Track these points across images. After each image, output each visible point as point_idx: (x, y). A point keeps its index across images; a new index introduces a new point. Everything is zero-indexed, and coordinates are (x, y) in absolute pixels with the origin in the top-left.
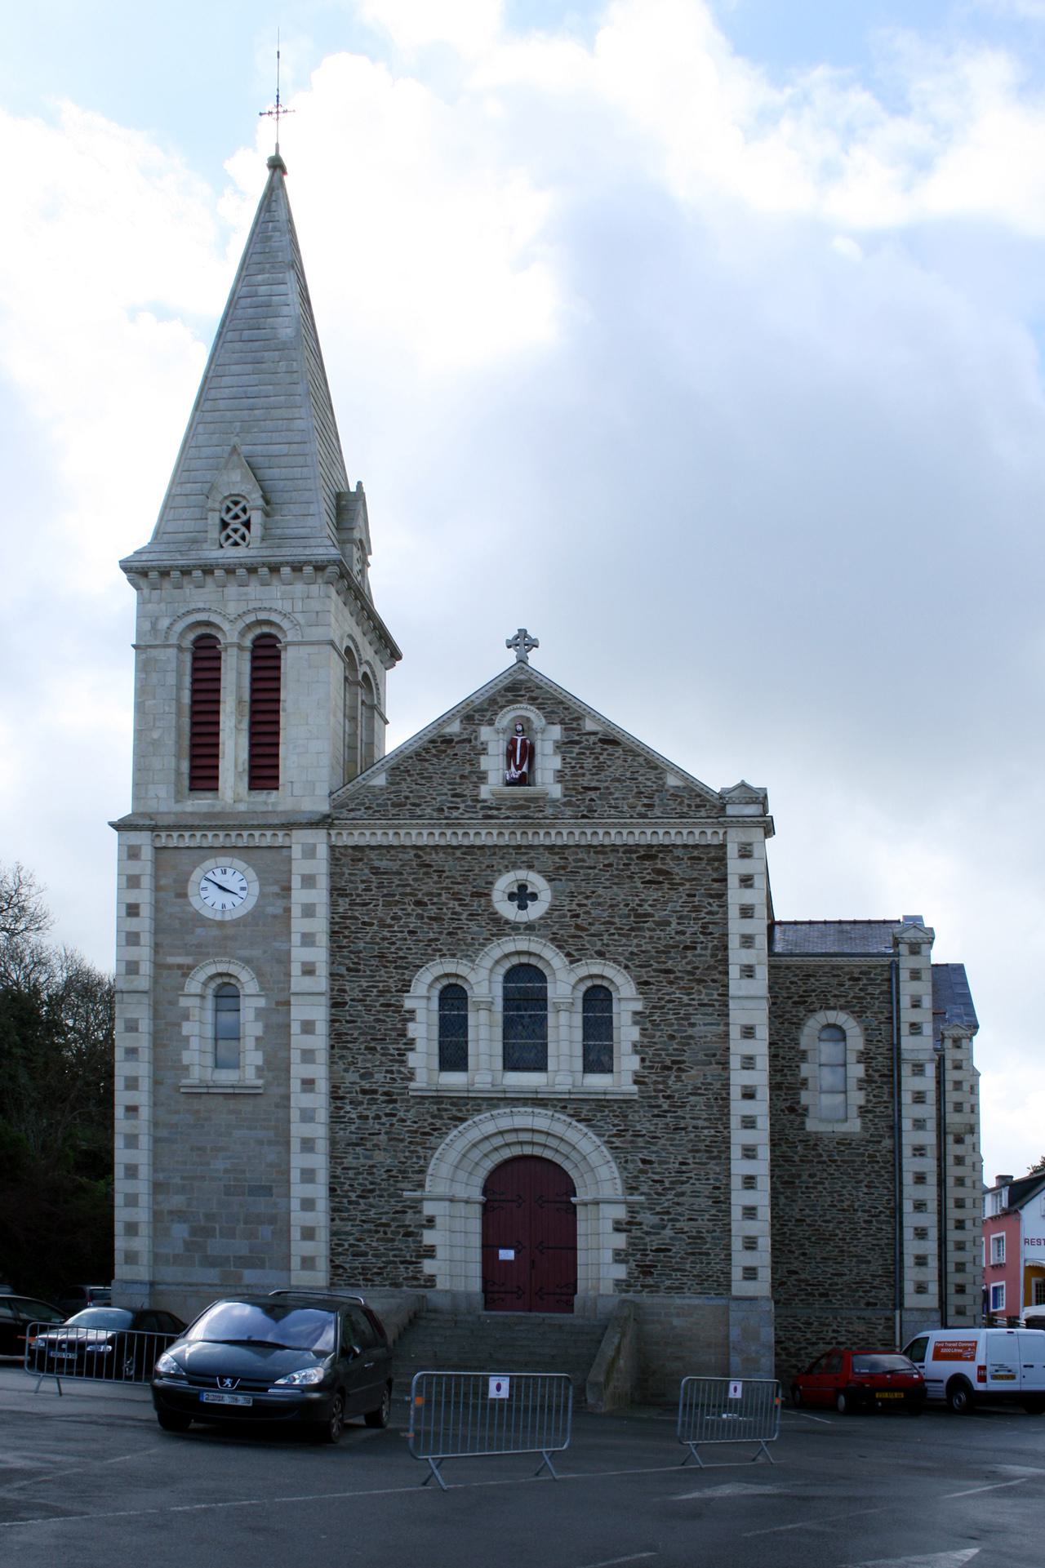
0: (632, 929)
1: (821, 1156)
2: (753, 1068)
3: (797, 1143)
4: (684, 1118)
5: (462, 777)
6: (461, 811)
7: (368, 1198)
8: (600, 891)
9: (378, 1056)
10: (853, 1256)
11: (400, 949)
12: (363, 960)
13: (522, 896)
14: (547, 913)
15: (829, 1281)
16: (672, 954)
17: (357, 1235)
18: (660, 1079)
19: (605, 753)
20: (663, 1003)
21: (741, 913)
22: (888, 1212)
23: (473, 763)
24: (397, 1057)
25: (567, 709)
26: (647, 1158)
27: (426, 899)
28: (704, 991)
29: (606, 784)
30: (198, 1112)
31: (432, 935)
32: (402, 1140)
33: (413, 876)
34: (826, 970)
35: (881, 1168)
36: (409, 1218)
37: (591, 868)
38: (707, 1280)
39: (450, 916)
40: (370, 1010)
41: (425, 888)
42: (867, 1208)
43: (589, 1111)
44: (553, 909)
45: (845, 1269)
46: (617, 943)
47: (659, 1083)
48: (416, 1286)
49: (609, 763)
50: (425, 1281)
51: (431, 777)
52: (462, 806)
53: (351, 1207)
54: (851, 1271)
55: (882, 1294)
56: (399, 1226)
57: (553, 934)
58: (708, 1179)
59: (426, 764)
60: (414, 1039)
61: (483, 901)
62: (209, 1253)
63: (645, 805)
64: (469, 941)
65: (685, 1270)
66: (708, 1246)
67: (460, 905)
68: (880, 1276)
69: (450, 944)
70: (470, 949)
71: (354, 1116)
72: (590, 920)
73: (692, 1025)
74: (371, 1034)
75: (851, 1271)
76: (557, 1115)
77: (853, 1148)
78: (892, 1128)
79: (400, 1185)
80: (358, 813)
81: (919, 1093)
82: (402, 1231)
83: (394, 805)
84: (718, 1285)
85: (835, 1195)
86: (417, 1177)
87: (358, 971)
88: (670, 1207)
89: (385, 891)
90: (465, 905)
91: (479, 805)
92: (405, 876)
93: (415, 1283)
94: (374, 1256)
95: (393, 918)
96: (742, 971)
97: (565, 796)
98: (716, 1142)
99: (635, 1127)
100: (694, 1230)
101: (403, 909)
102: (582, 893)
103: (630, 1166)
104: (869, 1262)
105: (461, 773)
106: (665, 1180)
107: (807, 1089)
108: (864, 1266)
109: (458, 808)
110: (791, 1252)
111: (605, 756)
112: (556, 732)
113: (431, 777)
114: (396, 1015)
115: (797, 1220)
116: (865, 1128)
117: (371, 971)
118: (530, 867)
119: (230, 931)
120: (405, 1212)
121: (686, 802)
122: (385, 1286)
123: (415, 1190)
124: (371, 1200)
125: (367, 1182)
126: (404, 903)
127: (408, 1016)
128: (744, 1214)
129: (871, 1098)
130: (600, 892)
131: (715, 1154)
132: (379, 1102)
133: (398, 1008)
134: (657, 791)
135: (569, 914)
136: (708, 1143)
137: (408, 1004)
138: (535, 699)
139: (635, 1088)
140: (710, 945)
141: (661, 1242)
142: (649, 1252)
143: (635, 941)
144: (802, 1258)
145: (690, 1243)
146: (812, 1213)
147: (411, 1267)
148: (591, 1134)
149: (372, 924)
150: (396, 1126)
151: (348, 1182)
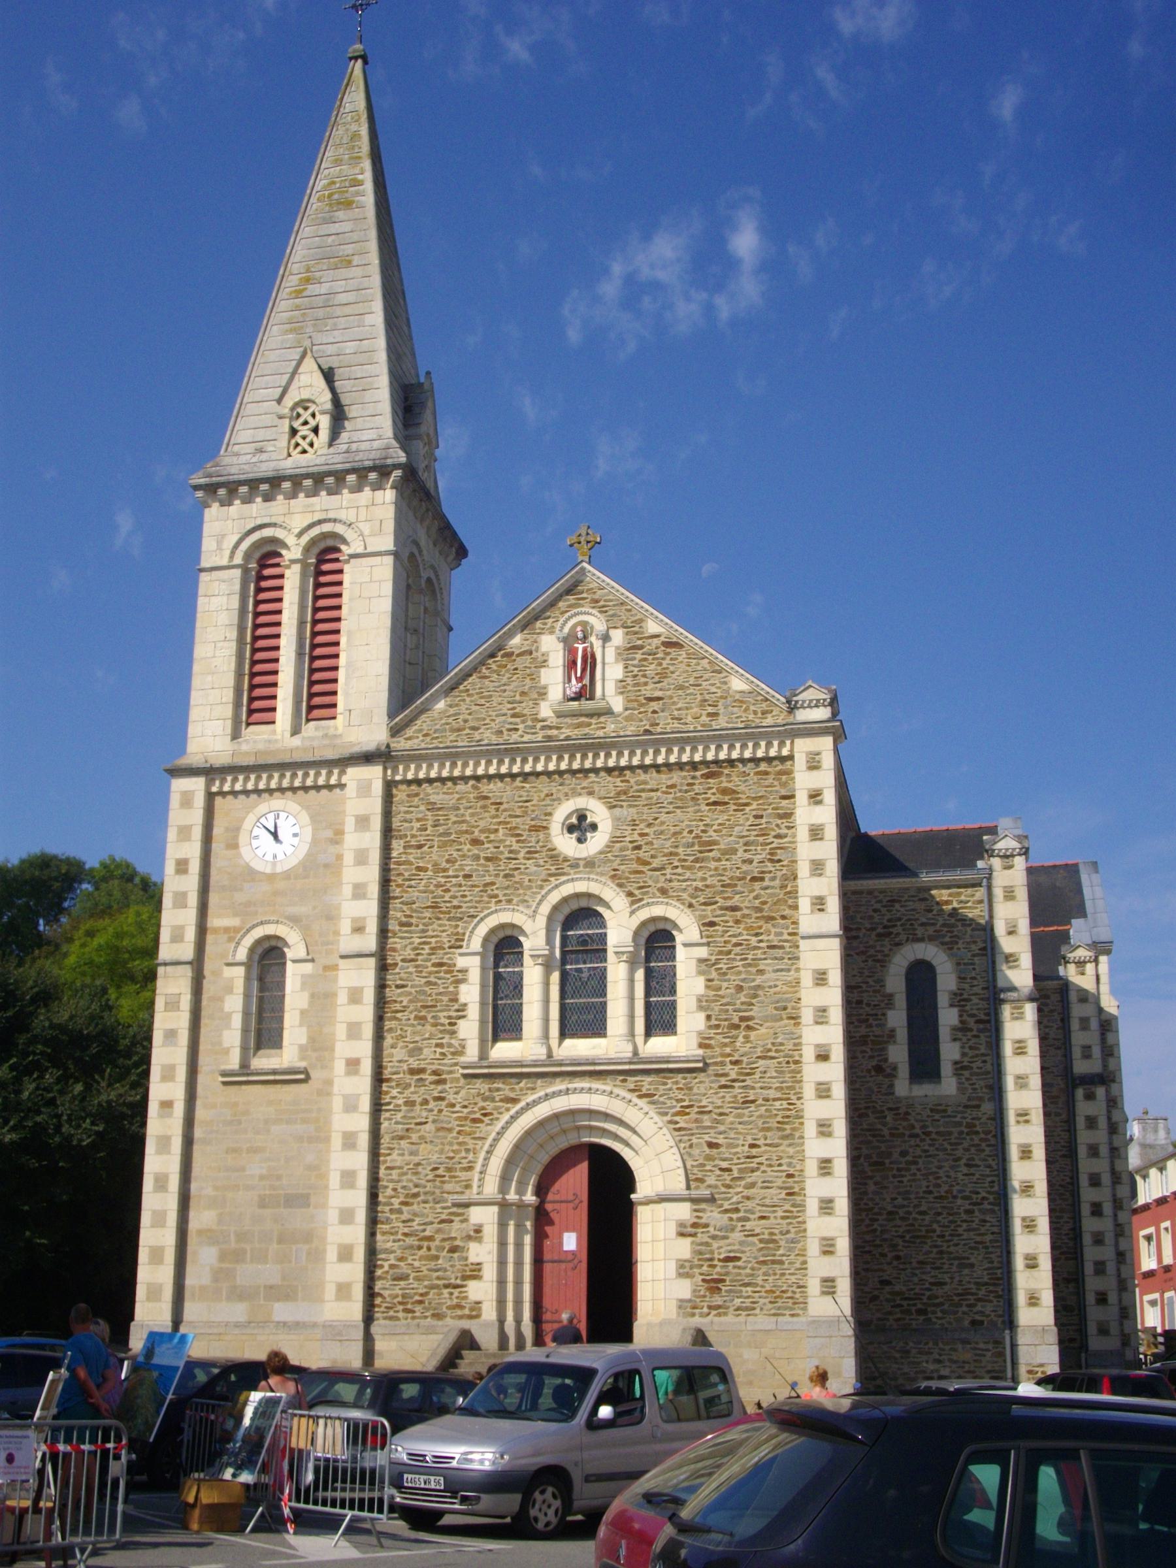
0: (697, 860)
1: (913, 1127)
2: (827, 1023)
3: (887, 1113)
4: (753, 1088)
5: (523, 694)
6: (520, 732)
7: (412, 1204)
8: (663, 817)
9: (428, 1027)
10: (954, 1259)
11: (454, 897)
12: (416, 911)
13: (580, 826)
14: (608, 846)
15: (928, 1293)
17: (399, 1253)
18: (727, 1040)
19: (668, 658)
20: (729, 947)
21: (811, 835)
22: (991, 1197)
23: (534, 677)
24: (448, 1027)
25: (629, 610)
26: (715, 1141)
27: (482, 837)
28: (773, 930)
29: (668, 693)
30: (236, 1104)
31: (488, 879)
32: (450, 1130)
33: (470, 811)
34: (913, 893)
35: (981, 1140)
36: (456, 1229)
37: (652, 790)
38: (782, 1297)
39: (507, 855)
40: (421, 972)
41: (482, 824)
42: (967, 1194)
43: (650, 1083)
44: (615, 840)
45: (945, 1276)
46: (681, 878)
47: (725, 1045)
48: (461, 1317)
49: (672, 668)
50: (472, 1309)
51: (491, 696)
52: (521, 726)
53: (393, 1216)
54: (952, 1278)
55: (988, 1308)
56: (444, 1240)
57: (615, 870)
58: (780, 1165)
59: (486, 682)
61: (541, 835)
62: (238, 1282)
63: (709, 715)
64: (527, 883)
65: (756, 1285)
66: (781, 1252)
67: (518, 842)
68: (987, 1284)
70: (528, 893)
71: (400, 1102)
72: (652, 852)
73: (761, 972)
74: (422, 1001)
75: (952, 1278)
76: (616, 1091)
77: (949, 1116)
78: (990, 1087)
79: (448, 1187)
80: (416, 741)
81: (1019, 1042)
82: (447, 1245)
83: (453, 730)
84: (795, 1303)
85: (931, 1178)
86: (463, 1175)
87: (410, 925)
88: (738, 1203)
90: (523, 842)
91: (539, 725)
92: (462, 811)
93: (459, 1312)
94: (417, 1279)
95: (448, 861)
96: (813, 904)
98: (788, 1117)
99: (700, 1101)
100: (766, 1232)
101: (458, 850)
102: (644, 820)
103: (696, 1152)
104: (972, 1266)
105: (521, 689)
106: (734, 1167)
107: (895, 1042)
108: (966, 1271)
109: (517, 730)
110: (883, 1255)
111: (667, 661)
112: (618, 636)
114: (448, 976)
115: (890, 1213)
116: (961, 1089)
118: (591, 793)
119: (281, 885)
120: (452, 1221)
121: (752, 708)
124: (415, 1207)
125: (411, 1185)
126: (461, 844)
127: (460, 976)
128: (821, 1208)
129: (967, 1050)
130: (662, 819)
131: (788, 1132)
132: (427, 1083)
133: (449, 967)
134: (721, 697)
135: (631, 846)
136: (779, 1119)
137: (461, 962)
138: (597, 601)
140: (779, 874)
141: (729, 1248)
142: (716, 1262)
143: (700, 874)
144: (895, 1263)
145: (761, 1249)
146: (905, 1203)
147: (456, 1292)
148: (652, 1114)
149: (426, 870)
150: (444, 1113)
151: (391, 1185)
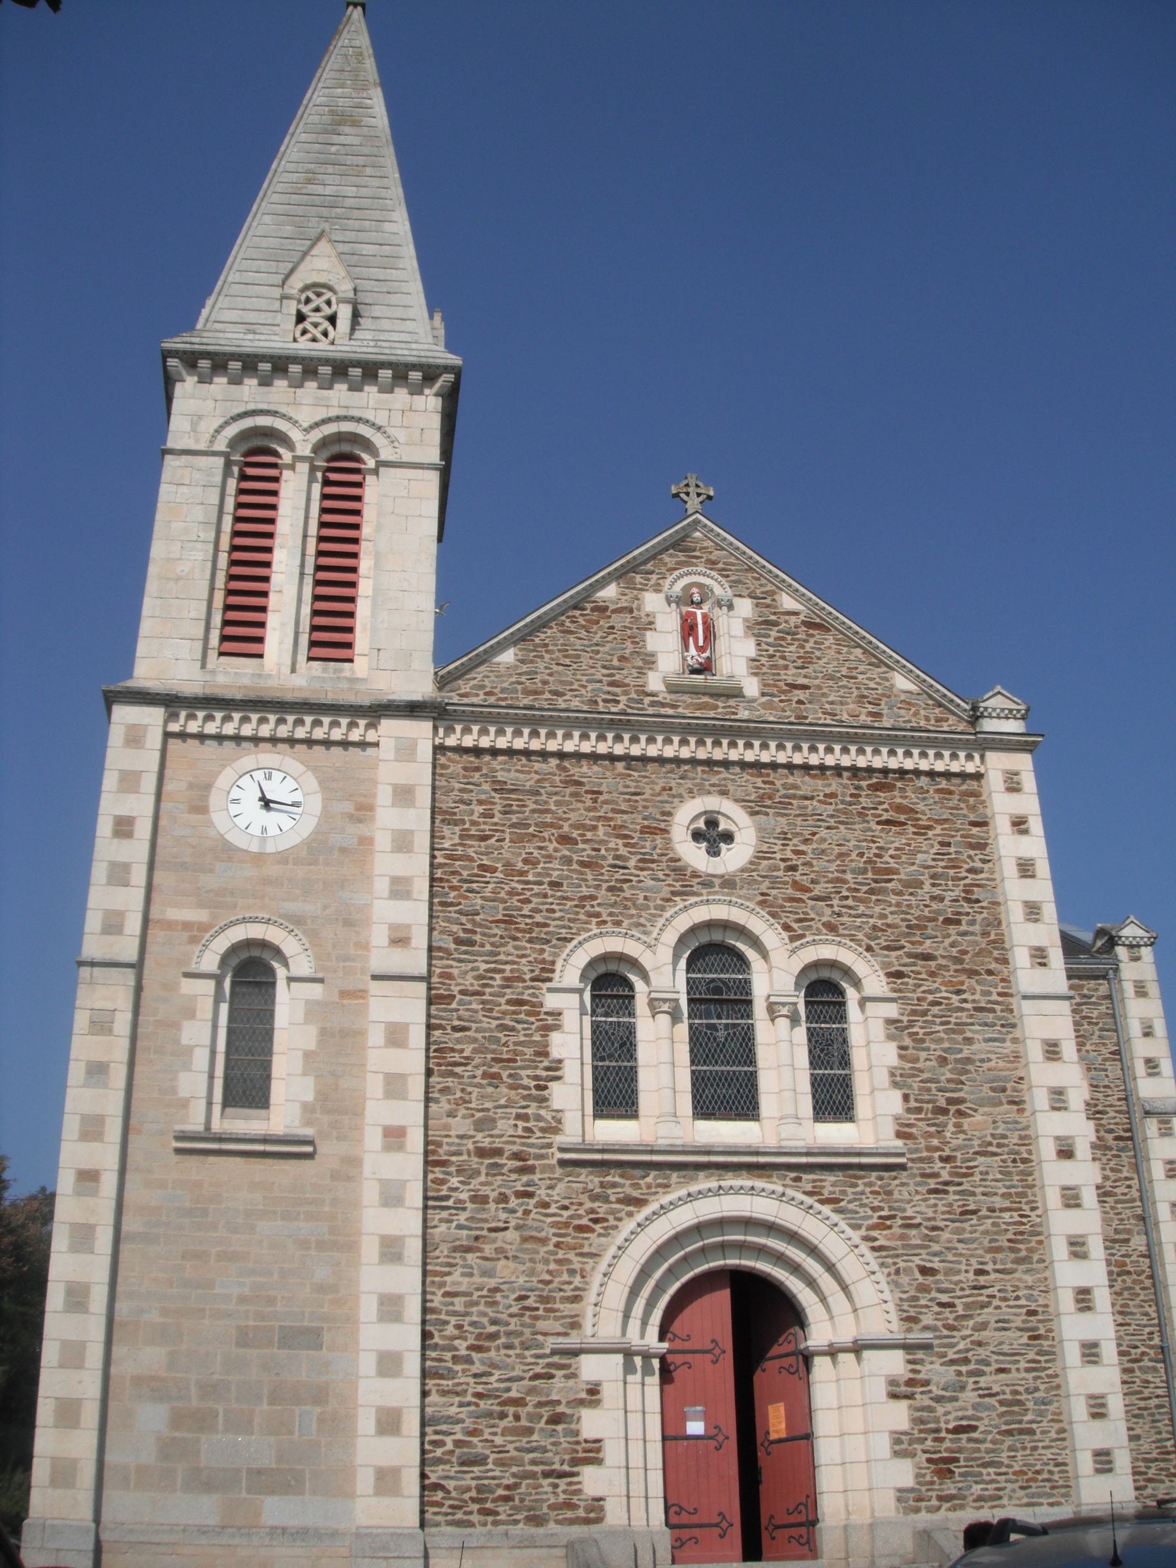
0: (871, 891)
4: (973, 1194)
5: (622, 658)
7: (488, 1349)
8: (823, 833)
9: (504, 1090)
12: (480, 925)
14: (751, 863)
16: (929, 931)
17: (469, 1424)
18: (933, 1129)
19: (812, 640)
23: (637, 641)
24: (534, 1092)
26: (929, 1265)
27: (575, 834)
28: (978, 988)
29: (817, 682)
31: (585, 891)
32: (544, 1241)
33: (555, 798)
36: (558, 1388)
37: (806, 798)
40: (491, 1010)
41: (573, 816)
44: (761, 856)
47: (929, 1135)
49: (818, 653)
51: (578, 656)
52: (623, 698)
53: (458, 1368)
56: (540, 1404)
57: (763, 894)
58: (1017, 1298)
59: (572, 638)
60: (560, 1061)
61: (659, 840)
63: (871, 714)
64: (641, 901)
67: (626, 845)
69: (612, 905)
70: (643, 914)
71: (464, 1196)
72: (813, 876)
73: (969, 1041)
74: (493, 1051)
79: (542, 1325)
82: (546, 1412)
86: (567, 1308)
87: (472, 943)
88: (967, 1350)
89: (514, 818)
90: (633, 846)
91: (647, 700)
92: (544, 797)
93: (569, 1514)
94: (499, 1463)
95: (525, 861)
97: (763, 695)
98: (1022, 1233)
99: (904, 1210)
100: (1008, 1390)
101: (541, 848)
103: (904, 1279)
105: (620, 653)
106: (957, 1301)
113: (578, 656)
114: (532, 1019)
117: (492, 944)
118: (724, 793)
119: (273, 870)
120: (552, 1376)
121: (922, 712)
122: (516, 1522)
123: (566, 1334)
124: (493, 1353)
125: (485, 1320)
126: (544, 839)
127: (550, 1021)
131: (1023, 1253)
132: (505, 1170)
133: (535, 1008)
134: (884, 695)
135: (782, 865)
136: (1010, 1236)
137: (551, 1001)
138: (714, 563)
139: (899, 1143)
141: (960, 1414)
142: (943, 1434)
143: (877, 909)
145: (1002, 1414)
147: (562, 1483)
149: (494, 870)
150: (532, 1216)
151: (453, 1320)
